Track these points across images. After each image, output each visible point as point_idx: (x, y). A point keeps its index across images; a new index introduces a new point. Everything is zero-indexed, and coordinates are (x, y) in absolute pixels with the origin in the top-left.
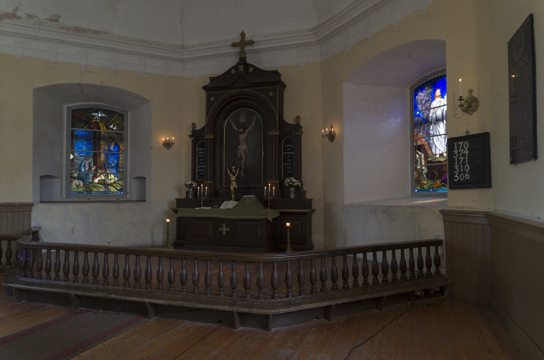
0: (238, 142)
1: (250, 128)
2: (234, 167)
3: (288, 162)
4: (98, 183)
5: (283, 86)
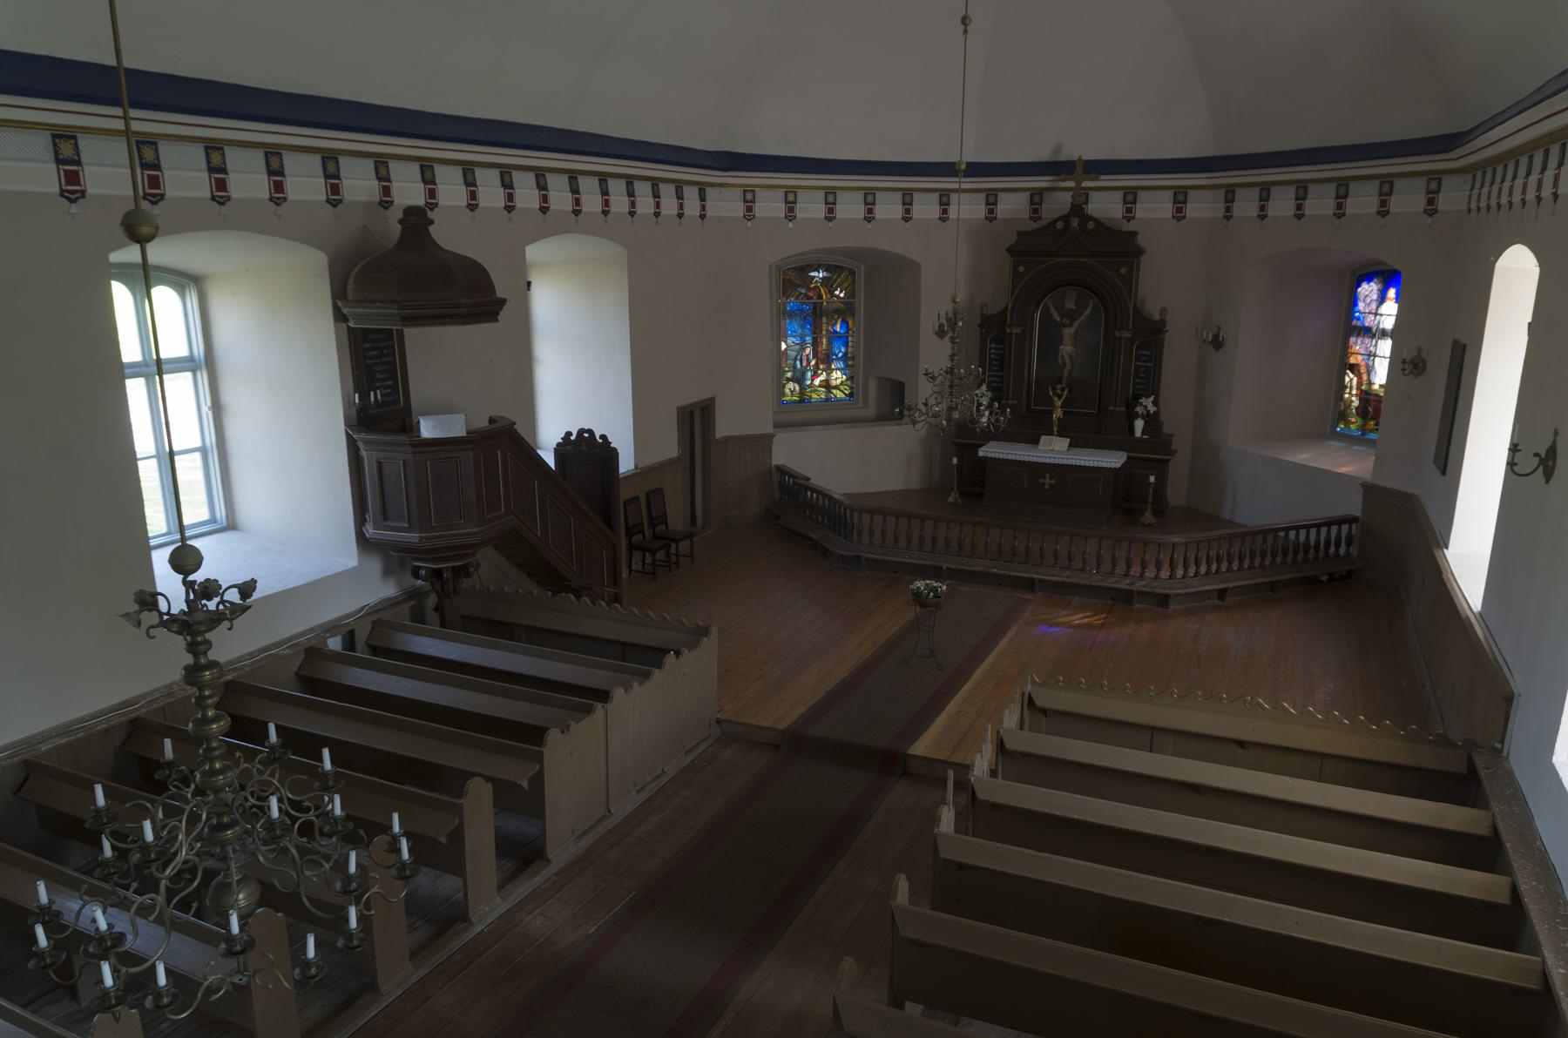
0: (1060, 340)
1: (1082, 318)
2: (1059, 386)
3: (1141, 378)
4: (820, 386)
5: (1138, 252)
